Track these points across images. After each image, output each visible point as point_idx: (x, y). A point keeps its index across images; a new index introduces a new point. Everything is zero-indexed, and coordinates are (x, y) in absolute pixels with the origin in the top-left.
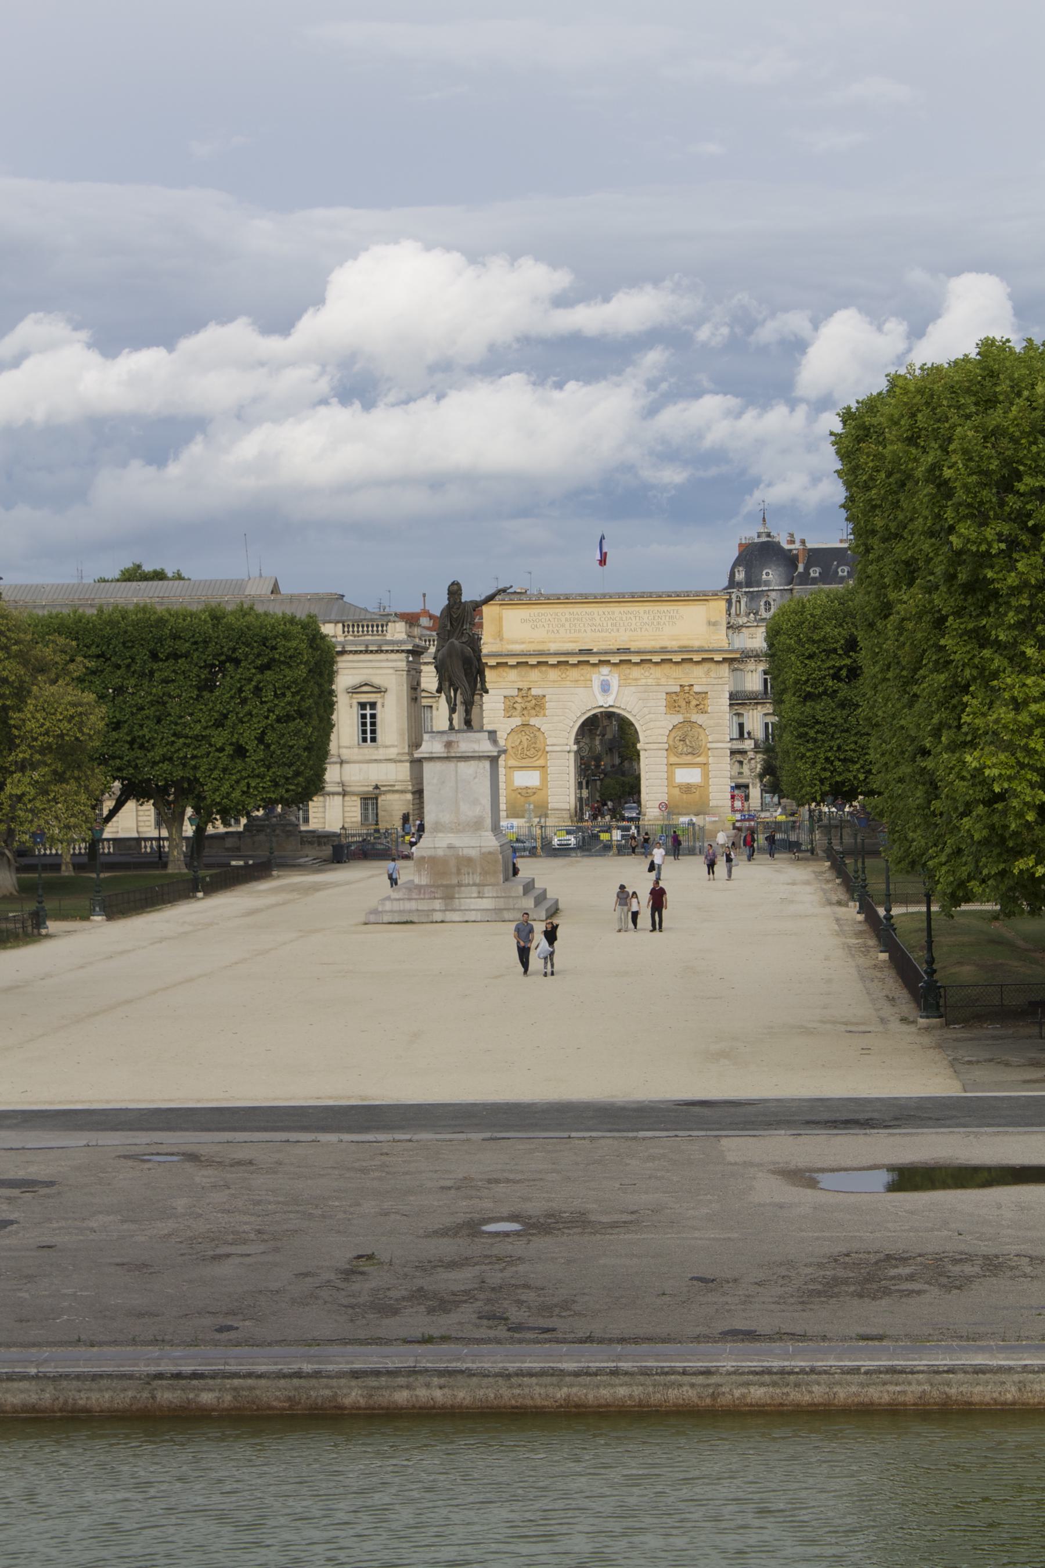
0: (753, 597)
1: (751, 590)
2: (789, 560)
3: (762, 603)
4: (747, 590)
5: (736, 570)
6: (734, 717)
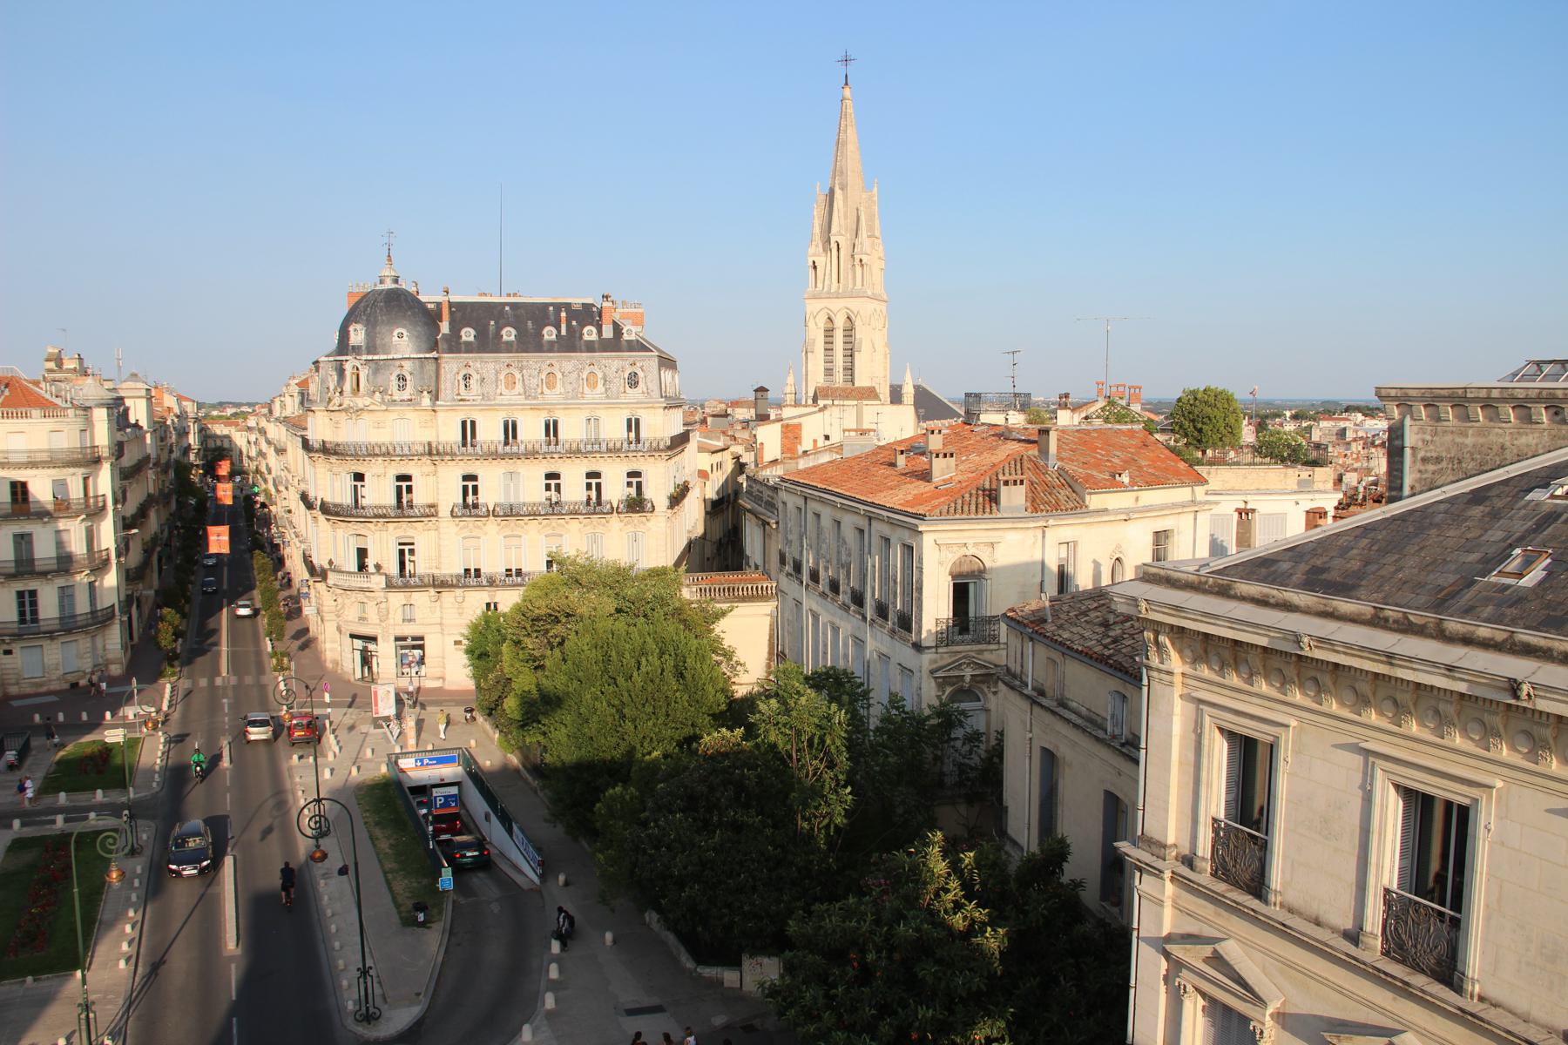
0: (377, 368)
1: (376, 357)
2: (428, 317)
3: (394, 377)
4: (370, 357)
5: (351, 329)
6: (351, 538)
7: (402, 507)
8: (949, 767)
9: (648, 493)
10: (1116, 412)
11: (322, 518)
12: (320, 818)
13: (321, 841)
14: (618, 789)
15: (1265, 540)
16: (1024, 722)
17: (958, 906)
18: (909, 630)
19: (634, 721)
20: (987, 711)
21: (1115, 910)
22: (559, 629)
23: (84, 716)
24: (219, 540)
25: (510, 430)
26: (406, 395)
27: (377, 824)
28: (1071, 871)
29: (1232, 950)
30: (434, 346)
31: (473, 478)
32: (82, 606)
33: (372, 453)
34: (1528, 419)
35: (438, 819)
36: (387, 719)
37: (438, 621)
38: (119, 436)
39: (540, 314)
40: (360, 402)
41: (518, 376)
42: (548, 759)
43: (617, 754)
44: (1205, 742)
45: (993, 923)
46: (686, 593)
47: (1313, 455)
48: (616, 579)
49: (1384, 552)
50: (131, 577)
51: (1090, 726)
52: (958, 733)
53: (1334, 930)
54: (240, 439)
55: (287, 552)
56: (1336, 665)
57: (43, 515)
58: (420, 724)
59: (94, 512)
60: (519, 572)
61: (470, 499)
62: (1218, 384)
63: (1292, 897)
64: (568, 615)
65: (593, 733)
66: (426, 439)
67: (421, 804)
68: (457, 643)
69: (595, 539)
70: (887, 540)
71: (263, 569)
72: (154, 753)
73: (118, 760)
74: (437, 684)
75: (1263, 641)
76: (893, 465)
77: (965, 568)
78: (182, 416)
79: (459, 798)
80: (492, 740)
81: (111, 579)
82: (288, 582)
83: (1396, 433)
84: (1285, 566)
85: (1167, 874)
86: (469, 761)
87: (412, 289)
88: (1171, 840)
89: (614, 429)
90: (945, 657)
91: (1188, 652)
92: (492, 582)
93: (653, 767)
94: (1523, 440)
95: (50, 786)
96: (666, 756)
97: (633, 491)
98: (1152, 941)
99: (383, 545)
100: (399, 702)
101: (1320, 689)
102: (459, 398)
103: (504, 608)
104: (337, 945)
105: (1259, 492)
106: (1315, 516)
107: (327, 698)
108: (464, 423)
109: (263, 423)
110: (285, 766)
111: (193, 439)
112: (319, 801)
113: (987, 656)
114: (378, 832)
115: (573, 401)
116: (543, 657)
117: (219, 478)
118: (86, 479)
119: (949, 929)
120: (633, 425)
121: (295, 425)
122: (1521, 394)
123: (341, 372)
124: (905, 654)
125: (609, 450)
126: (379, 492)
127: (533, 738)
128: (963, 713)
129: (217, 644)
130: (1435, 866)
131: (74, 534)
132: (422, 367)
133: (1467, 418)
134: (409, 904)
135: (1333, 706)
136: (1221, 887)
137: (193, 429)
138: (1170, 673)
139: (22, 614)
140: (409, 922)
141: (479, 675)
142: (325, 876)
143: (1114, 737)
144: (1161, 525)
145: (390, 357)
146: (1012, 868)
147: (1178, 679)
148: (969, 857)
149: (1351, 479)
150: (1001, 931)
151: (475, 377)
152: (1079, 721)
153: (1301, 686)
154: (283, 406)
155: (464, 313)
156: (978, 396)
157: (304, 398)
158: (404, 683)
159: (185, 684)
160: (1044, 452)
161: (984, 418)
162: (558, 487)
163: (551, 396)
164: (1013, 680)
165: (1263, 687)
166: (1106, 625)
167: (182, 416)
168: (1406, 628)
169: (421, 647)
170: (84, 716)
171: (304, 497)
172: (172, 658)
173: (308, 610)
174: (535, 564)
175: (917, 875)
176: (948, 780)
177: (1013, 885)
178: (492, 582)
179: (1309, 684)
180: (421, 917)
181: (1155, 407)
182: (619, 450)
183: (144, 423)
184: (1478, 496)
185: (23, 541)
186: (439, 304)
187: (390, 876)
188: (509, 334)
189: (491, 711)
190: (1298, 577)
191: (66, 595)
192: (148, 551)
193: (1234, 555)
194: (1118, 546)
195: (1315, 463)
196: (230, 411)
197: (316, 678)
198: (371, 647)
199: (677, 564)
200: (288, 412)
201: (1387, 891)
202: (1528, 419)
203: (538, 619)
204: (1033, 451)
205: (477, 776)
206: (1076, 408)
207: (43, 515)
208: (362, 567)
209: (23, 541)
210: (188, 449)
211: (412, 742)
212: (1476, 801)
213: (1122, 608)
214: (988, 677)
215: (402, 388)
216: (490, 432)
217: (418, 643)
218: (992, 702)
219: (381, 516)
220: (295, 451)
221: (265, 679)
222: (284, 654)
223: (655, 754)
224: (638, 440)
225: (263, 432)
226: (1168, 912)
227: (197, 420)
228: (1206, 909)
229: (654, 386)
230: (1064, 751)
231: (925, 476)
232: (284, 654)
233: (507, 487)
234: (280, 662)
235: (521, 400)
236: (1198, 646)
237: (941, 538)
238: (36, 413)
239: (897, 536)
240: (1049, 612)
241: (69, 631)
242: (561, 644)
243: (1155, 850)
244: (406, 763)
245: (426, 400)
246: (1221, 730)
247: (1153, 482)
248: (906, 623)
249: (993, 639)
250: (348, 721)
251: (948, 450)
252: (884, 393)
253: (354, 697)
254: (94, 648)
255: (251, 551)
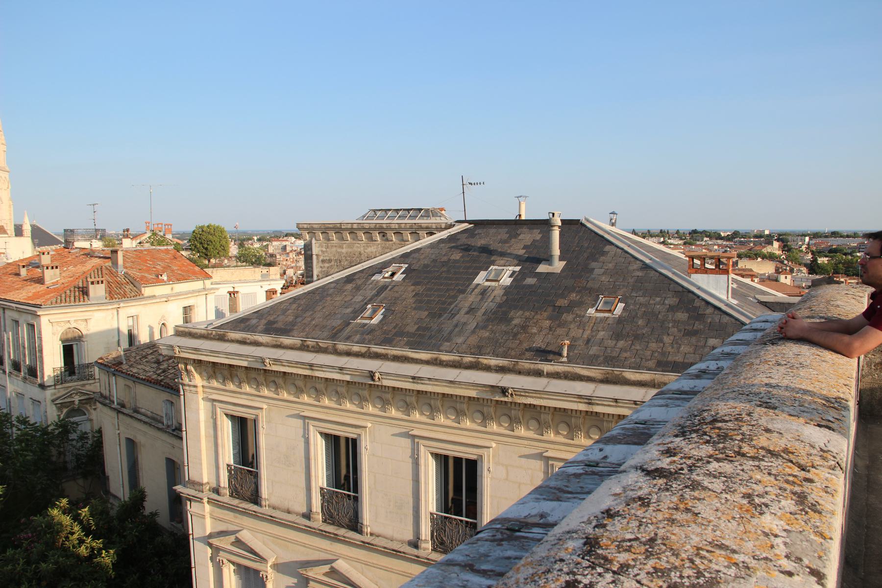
8: (69, 457)
10: (157, 239)
15: (244, 307)
16: (113, 424)
17: (81, 542)
18: (36, 376)
20: (91, 420)
21: (180, 526)
28: (149, 507)
29: (246, 536)
34: (371, 239)
44: (219, 423)
45: (106, 547)
47: (269, 260)
49: (305, 311)
51: (154, 422)
52: (74, 436)
53: (297, 514)
56: (285, 373)
62: (215, 222)
63: (274, 501)
70: (17, 322)
75: (245, 364)
76: (18, 275)
77: (70, 336)
83: (308, 248)
84: (254, 321)
85: (205, 500)
88: (205, 480)
90: (61, 391)
91: (205, 374)
94: (369, 250)
98: (199, 539)
101: (277, 387)
105: (240, 281)
106: (271, 293)
113: (88, 387)
119: (78, 557)
122: (367, 226)
124: (33, 391)
128: (77, 424)
130: (343, 472)
133: (343, 239)
135: (285, 395)
136: (236, 502)
138: (195, 386)
143: (168, 426)
144: (187, 303)
146: (113, 513)
147: (200, 389)
148: (85, 512)
149: (290, 272)
150: (112, 551)
152: (147, 420)
153: (267, 386)
156: (72, 231)
160: (115, 263)
161: (77, 244)
164: (105, 400)
165: (247, 388)
166: (158, 362)
168: (318, 350)
175: (53, 528)
176: (70, 466)
177: (116, 523)
179: (272, 384)
181: (181, 236)
184: (349, 279)
190: (260, 328)
193: (229, 317)
194: (163, 317)
195: (270, 265)
201: (322, 489)
202: (371, 239)
204: (109, 263)
206: (135, 237)
212: (359, 435)
213: (165, 352)
214: (90, 400)
218: (94, 415)
226: (208, 521)
228: (229, 515)
230: (140, 438)
231: (40, 281)
236: (210, 370)
237: (53, 318)
239: (23, 319)
240: (123, 358)
243: (198, 488)
246: (227, 415)
247: (181, 279)
248: (33, 372)
249: (91, 377)
251: (54, 265)
252: (11, 229)
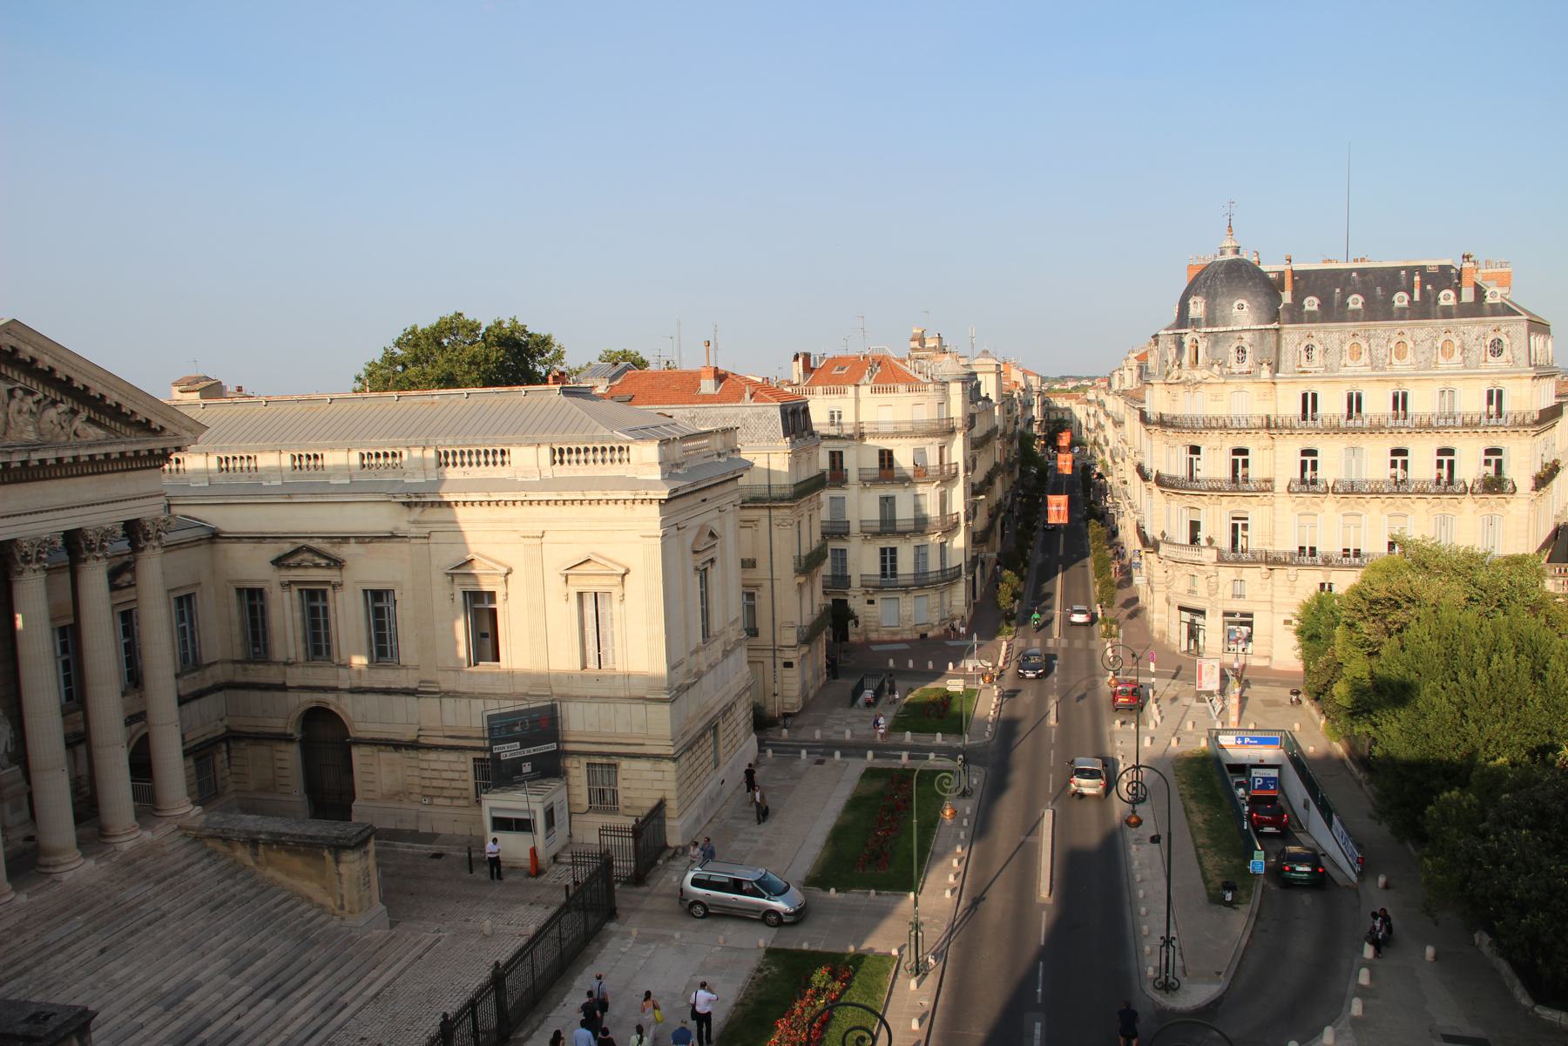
0: (1216, 340)
1: (1215, 330)
2: (1272, 287)
3: (1233, 349)
4: (1209, 330)
5: (1191, 302)
6: (1184, 510)
7: (1238, 481)
9: (1509, 472)
11: (1156, 490)
12: (1137, 782)
13: (1136, 806)
14: (1455, 793)
19: (1476, 721)
22: (1398, 615)
23: (930, 665)
24: (1057, 509)
25: (1354, 403)
26: (1245, 367)
27: (1193, 797)
30: (1275, 317)
31: (1313, 453)
32: (934, 565)
33: (1209, 425)
35: (1255, 802)
36: (1210, 694)
37: (1269, 598)
38: (972, 409)
39: (1390, 279)
40: (1198, 375)
41: (1364, 346)
42: (1377, 751)
43: (1456, 756)
46: (1550, 585)
48: (1467, 566)
50: (977, 539)
54: (1079, 412)
55: (1120, 522)
57: (905, 480)
58: (1243, 700)
59: (948, 479)
60: (1357, 553)
61: (1308, 475)
64: (1410, 600)
65: (1430, 730)
66: (1264, 412)
67: (1239, 785)
68: (1287, 622)
69: (1444, 521)
71: (1097, 537)
72: (988, 705)
73: (956, 708)
74: (1263, 663)
78: (1027, 390)
79: (1278, 782)
80: (1317, 725)
81: (959, 541)
82: (1120, 555)
86: (1290, 744)
87: (1254, 259)
89: (1471, 401)
92: (1327, 562)
93: (1498, 775)
95: (898, 725)
96: (1513, 764)
97: (1491, 470)
99: (1216, 518)
100: (1224, 677)
102: (1301, 369)
103: (1339, 589)
104: (1143, 910)
107: (1152, 668)
108: (1305, 396)
109: (1102, 396)
110: (1107, 730)
111: (1036, 412)
112: (1137, 767)
114: (1192, 805)
115: (1425, 371)
116: (1381, 644)
117: (1058, 449)
118: (941, 448)
120: (1495, 397)
121: (1133, 398)
123: (1180, 345)
125: (1465, 425)
126: (1214, 465)
127: (1362, 728)
129: (1051, 607)
131: (930, 497)
132: (1262, 338)
134: (1219, 881)
137: (1037, 401)
139: (884, 568)
140: (1216, 899)
141: (1309, 656)
142: (1138, 841)
145: (1229, 329)
151: (1318, 347)
154: (1122, 379)
155: (1307, 282)
157: (1143, 372)
158: (1229, 659)
159: (1019, 643)
162: (1405, 465)
163: (1400, 366)
167: (1027, 390)
169: (1250, 624)
170: (930, 665)
171: (1140, 469)
172: (1009, 617)
173: (1139, 580)
174: (1375, 546)
178: (1327, 562)
180: (1229, 896)
182: (1477, 425)
183: (993, 397)
185: (887, 503)
186: (1281, 274)
187: (1201, 851)
188: (1356, 302)
189: (1318, 696)
191: (921, 552)
192: (992, 516)
196: (1070, 385)
197: (1142, 648)
198: (1199, 620)
199: (1539, 551)
200: (1126, 386)
203: (1375, 602)
205: (1299, 762)
207: (905, 480)
208: (1194, 540)
209: (887, 503)
210: (1031, 421)
211: (1234, 718)
215: (1241, 360)
216: (1332, 405)
217: (1247, 620)
219: (1215, 489)
220: (1132, 423)
221: (1094, 644)
222: (1112, 622)
223: (1500, 760)
224: (1499, 414)
225: (1102, 404)
227: (1040, 393)
229: (1522, 355)
232: (1112, 622)
233: (1349, 464)
234: (1109, 629)
235: (1367, 371)
238: (902, 388)
241: (921, 587)
242: (1400, 630)
244: (1224, 740)
245: (1265, 373)
250: (1171, 692)
253: (1179, 669)
254: (942, 603)
255: (1086, 519)
